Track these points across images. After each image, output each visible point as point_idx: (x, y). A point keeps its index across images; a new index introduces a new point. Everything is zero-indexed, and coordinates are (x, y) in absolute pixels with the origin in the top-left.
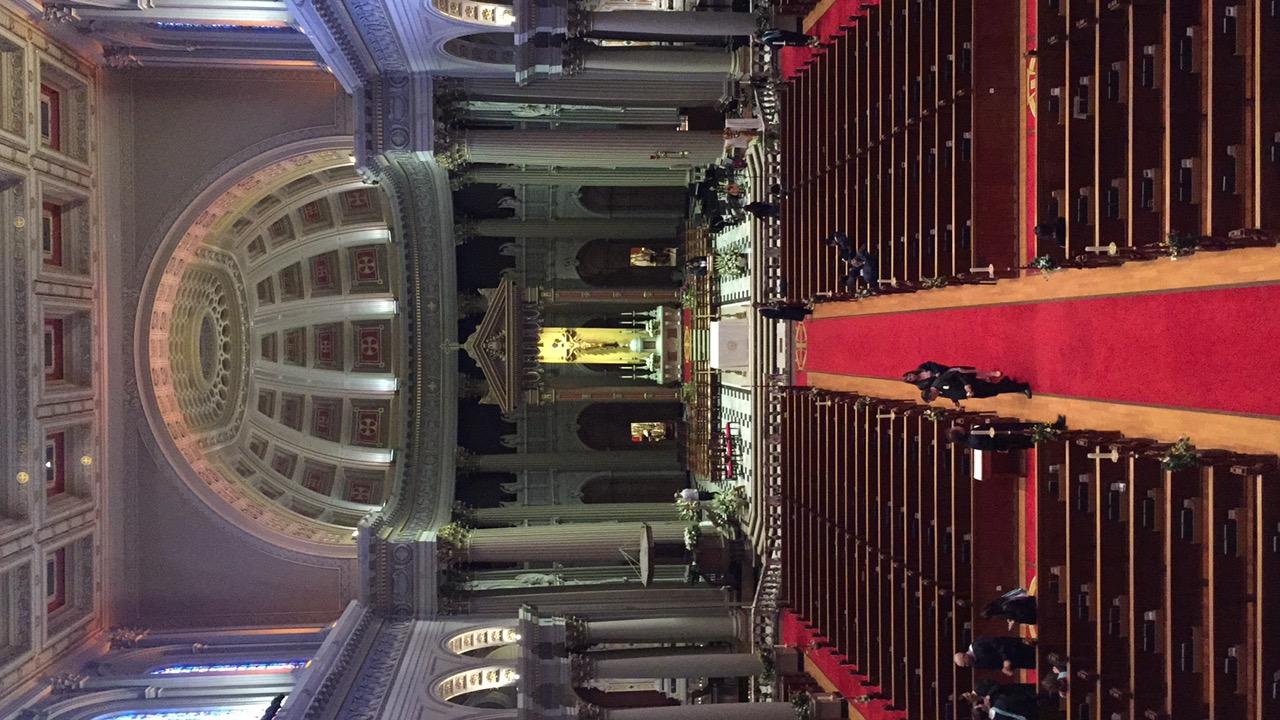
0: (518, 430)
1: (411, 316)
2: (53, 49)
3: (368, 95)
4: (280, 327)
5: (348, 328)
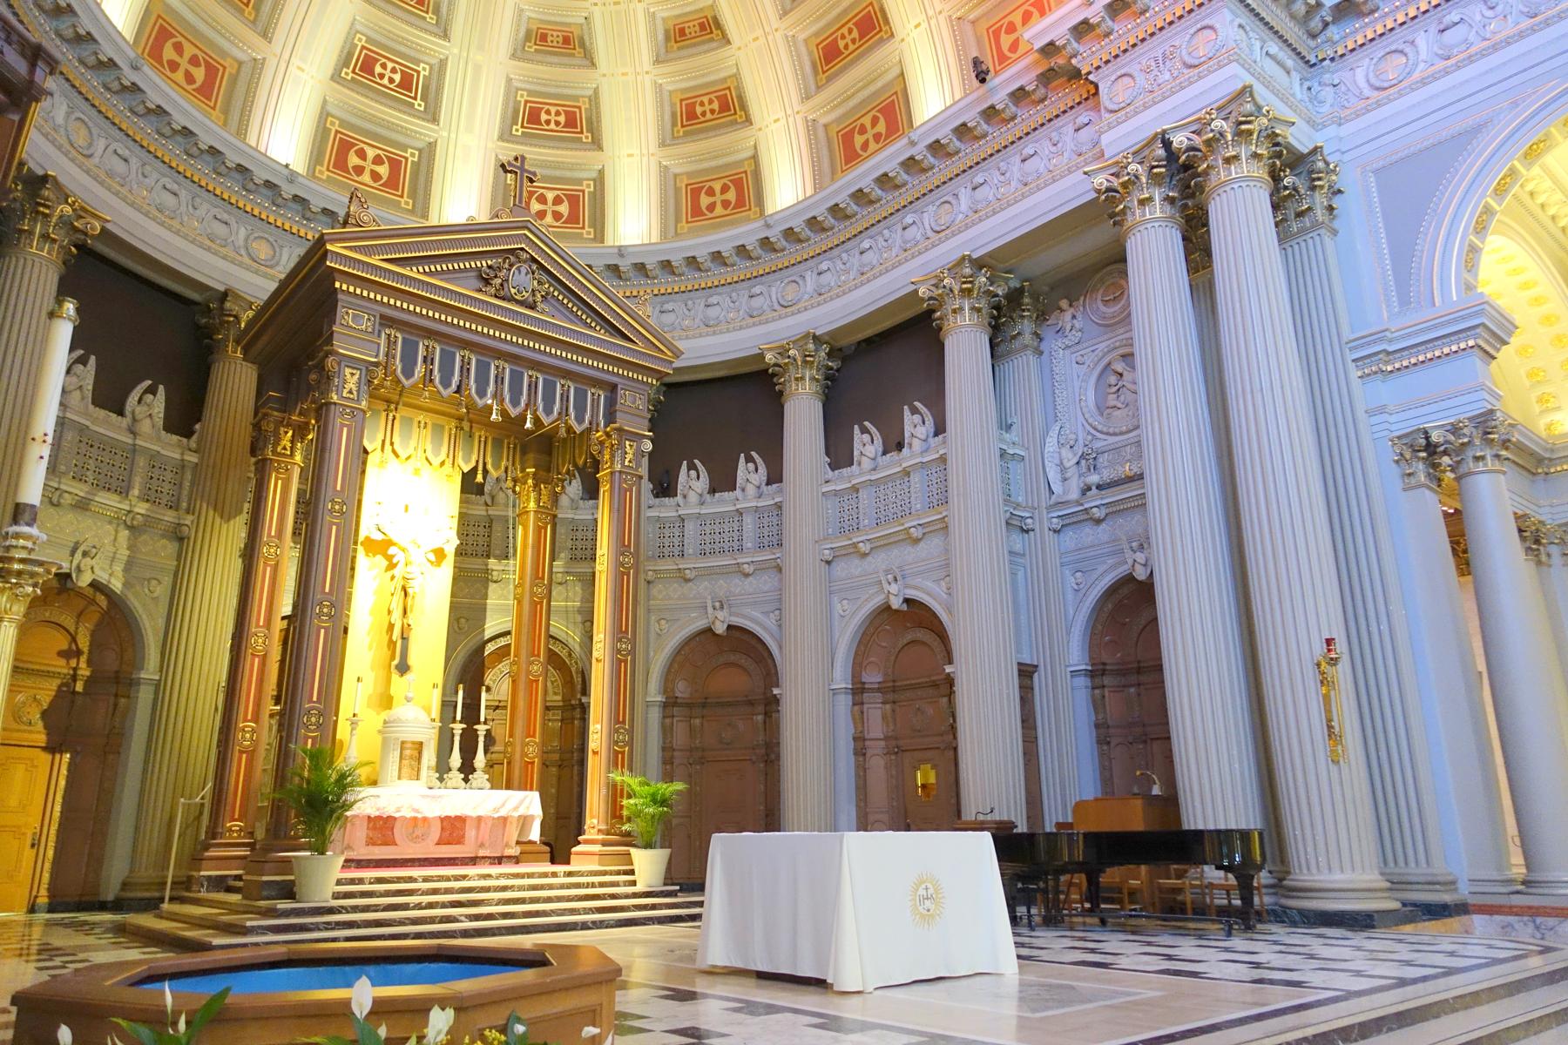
5: (588, 161)
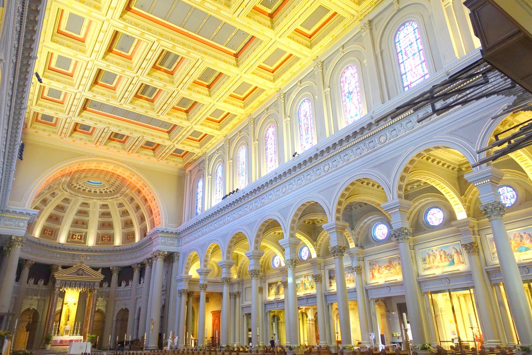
1: (87, 251)
2: (196, 157)
3: (176, 233)
4: (91, 210)
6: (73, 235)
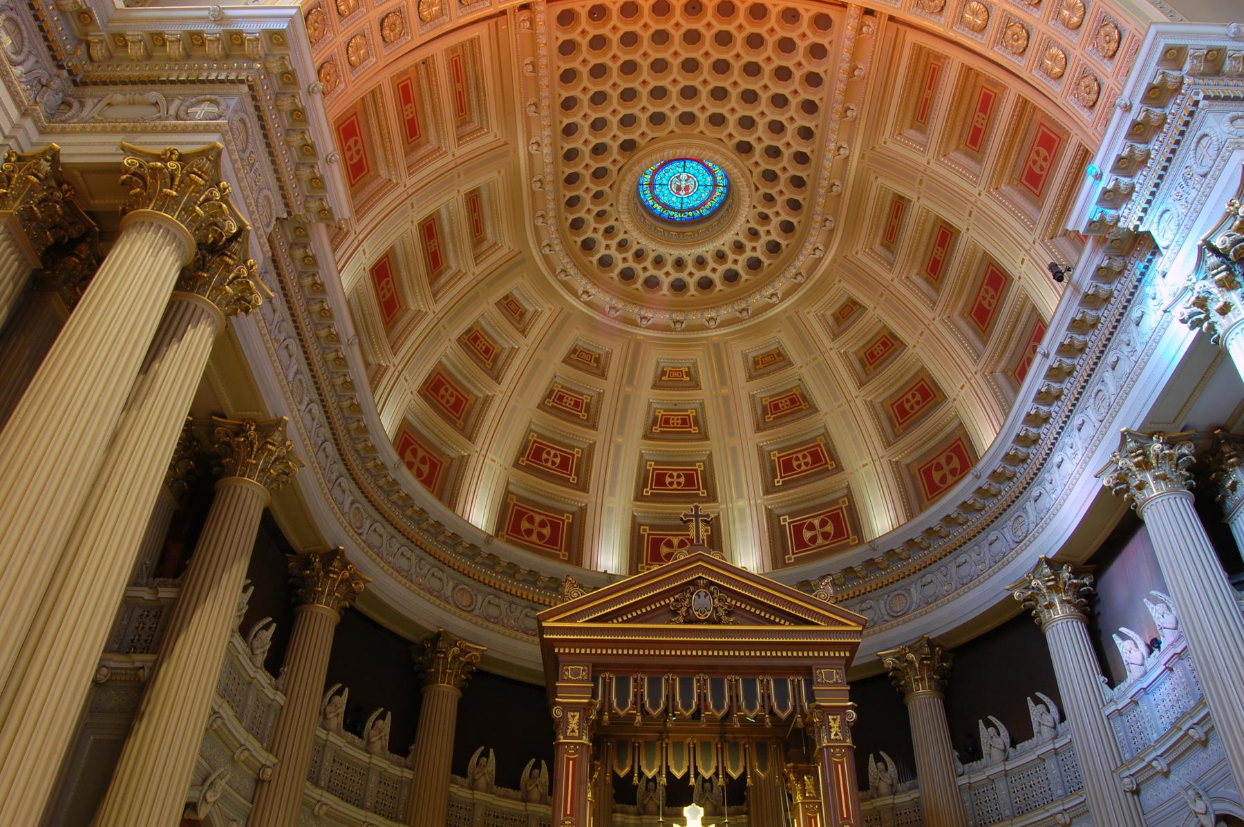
0: (502, 790)
6: (656, 543)
